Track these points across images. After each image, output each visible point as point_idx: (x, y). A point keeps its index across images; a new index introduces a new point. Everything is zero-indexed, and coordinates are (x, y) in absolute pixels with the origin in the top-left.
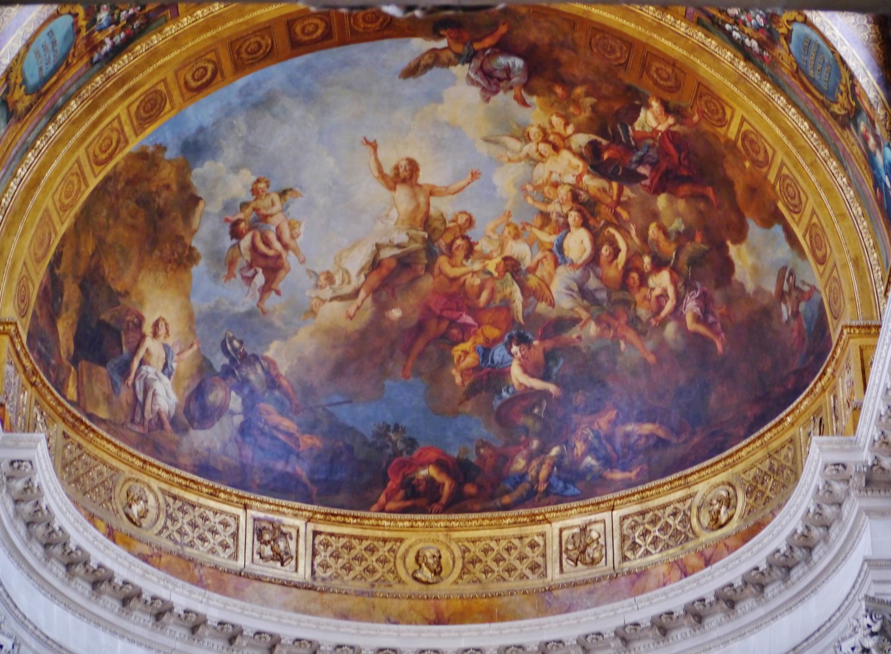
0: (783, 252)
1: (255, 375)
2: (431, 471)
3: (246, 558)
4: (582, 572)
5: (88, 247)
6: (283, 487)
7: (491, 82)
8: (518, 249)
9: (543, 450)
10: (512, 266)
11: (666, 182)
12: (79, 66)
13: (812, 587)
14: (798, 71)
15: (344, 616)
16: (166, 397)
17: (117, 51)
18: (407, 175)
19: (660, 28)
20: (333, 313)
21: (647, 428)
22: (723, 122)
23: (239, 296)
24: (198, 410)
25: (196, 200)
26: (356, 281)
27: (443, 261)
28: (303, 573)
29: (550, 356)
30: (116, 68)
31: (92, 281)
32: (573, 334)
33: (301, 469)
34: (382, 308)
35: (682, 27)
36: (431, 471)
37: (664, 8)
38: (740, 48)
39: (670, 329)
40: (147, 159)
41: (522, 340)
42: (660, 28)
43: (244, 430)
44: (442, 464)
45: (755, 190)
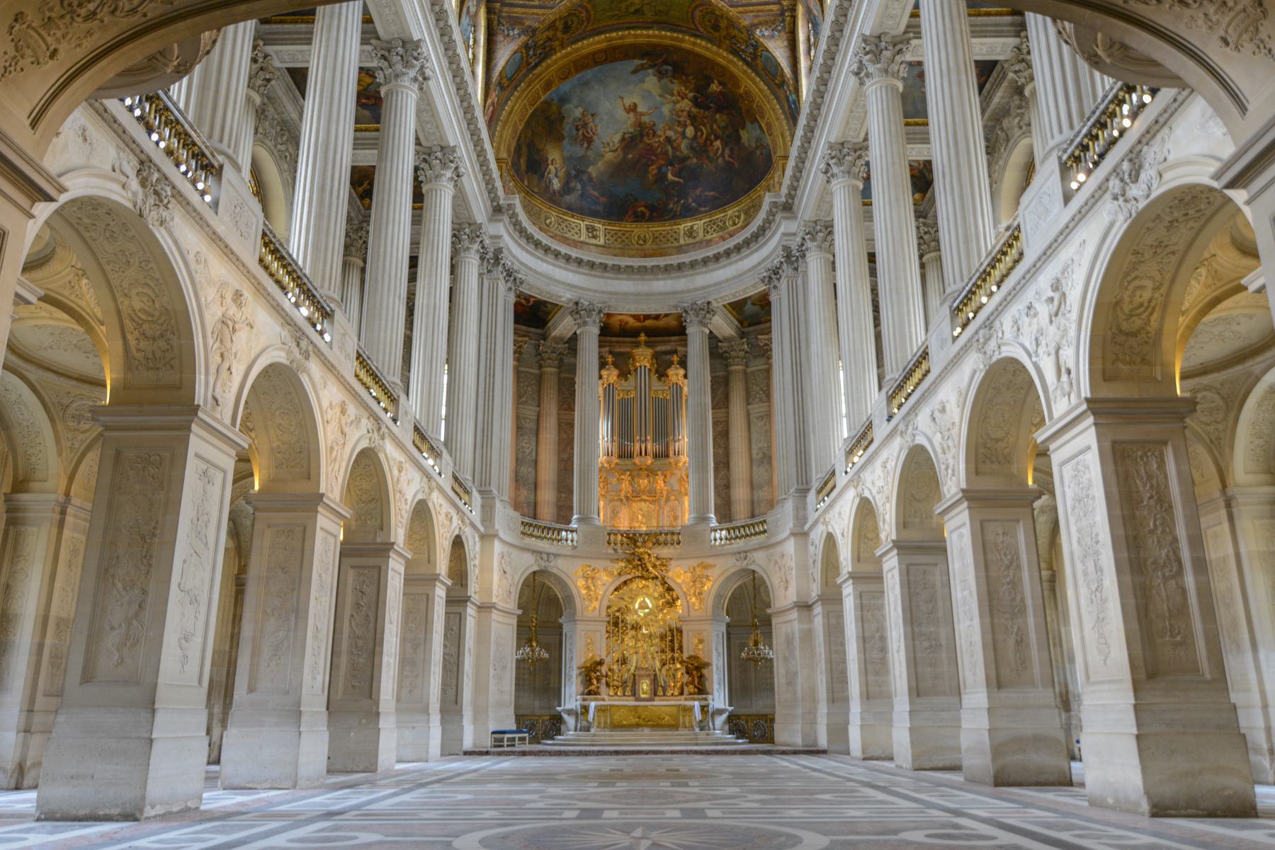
0: (758, 132)
1: (585, 178)
3: (584, 237)
4: (691, 241)
5: (530, 135)
6: (595, 214)
7: (661, 75)
8: (670, 133)
10: (668, 139)
11: (719, 109)
12: (524, 71)
13: (765, 244)
14: (765, 68)
16: (556, 184)
17: (536, 65)
18: (633, 109)
19: (718, 55)
20: (609, 156)
22: (739, 87)
23: (579, 151)
24: (566, 189)
25: (564, 118)
27: (645, 138)
28: (602, 242)
29: (681, 170)
31: (531, 146)
32: (689, 162)
33: (600, 208)
34: (625, 154)
37: (719, 47)
38: (744, 61)
39: (720, 160)
40: (545, 102)
41: (672, 165)
43: (582, 195)
44: (646, 207)
45: (749, 111)
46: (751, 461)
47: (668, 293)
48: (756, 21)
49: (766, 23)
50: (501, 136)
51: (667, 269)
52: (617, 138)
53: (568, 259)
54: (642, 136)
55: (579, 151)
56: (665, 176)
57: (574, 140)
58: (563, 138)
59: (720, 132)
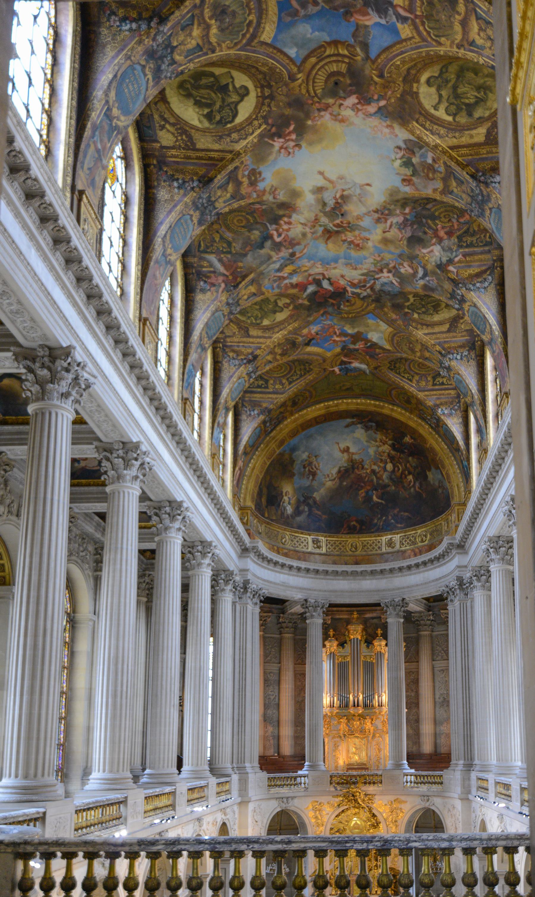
2: (354, 523)
5: (268, 478)
6: (318, 530)
8: (375, 467)
9: (381, 518)
10: (373, 471)
11: (411, 454)
15: (335, 563)
17: (272, 431)
20: (329, 484)
21: (406, 514)
23: (306, 482)
24: (297, 512)
26: (335, 476)
27: (356, 470)
28: (324, 550)
29: (383, 494)
30: (272, 434)
32: (388, 489)
34: (341, 482)
35: (415, 419)
36: (354, 523)
37: (411, 413)
38: (430, 425)
39: (412, 490)
40: (281, 455)
42: (410, 418)
43: (309, 515)
44: (357, 521)
46: (435, 702)
47: (374, 591)
48: (438, 402)
49: (446, 403)
50: (247, 488)
51: (373, 573)
52: (335, 471)
53: (299, 569)
54: (353, 468)
55: (306, 482)
56: (372, 498)
57: (302, 475)
58: (294, 475)
59: (412, 470)
